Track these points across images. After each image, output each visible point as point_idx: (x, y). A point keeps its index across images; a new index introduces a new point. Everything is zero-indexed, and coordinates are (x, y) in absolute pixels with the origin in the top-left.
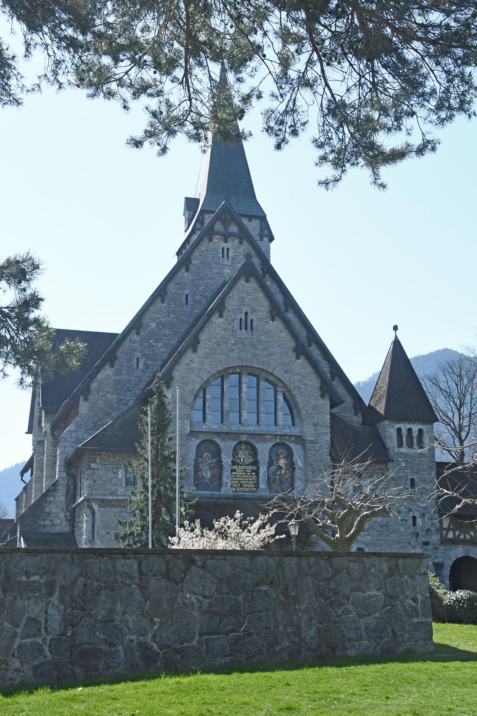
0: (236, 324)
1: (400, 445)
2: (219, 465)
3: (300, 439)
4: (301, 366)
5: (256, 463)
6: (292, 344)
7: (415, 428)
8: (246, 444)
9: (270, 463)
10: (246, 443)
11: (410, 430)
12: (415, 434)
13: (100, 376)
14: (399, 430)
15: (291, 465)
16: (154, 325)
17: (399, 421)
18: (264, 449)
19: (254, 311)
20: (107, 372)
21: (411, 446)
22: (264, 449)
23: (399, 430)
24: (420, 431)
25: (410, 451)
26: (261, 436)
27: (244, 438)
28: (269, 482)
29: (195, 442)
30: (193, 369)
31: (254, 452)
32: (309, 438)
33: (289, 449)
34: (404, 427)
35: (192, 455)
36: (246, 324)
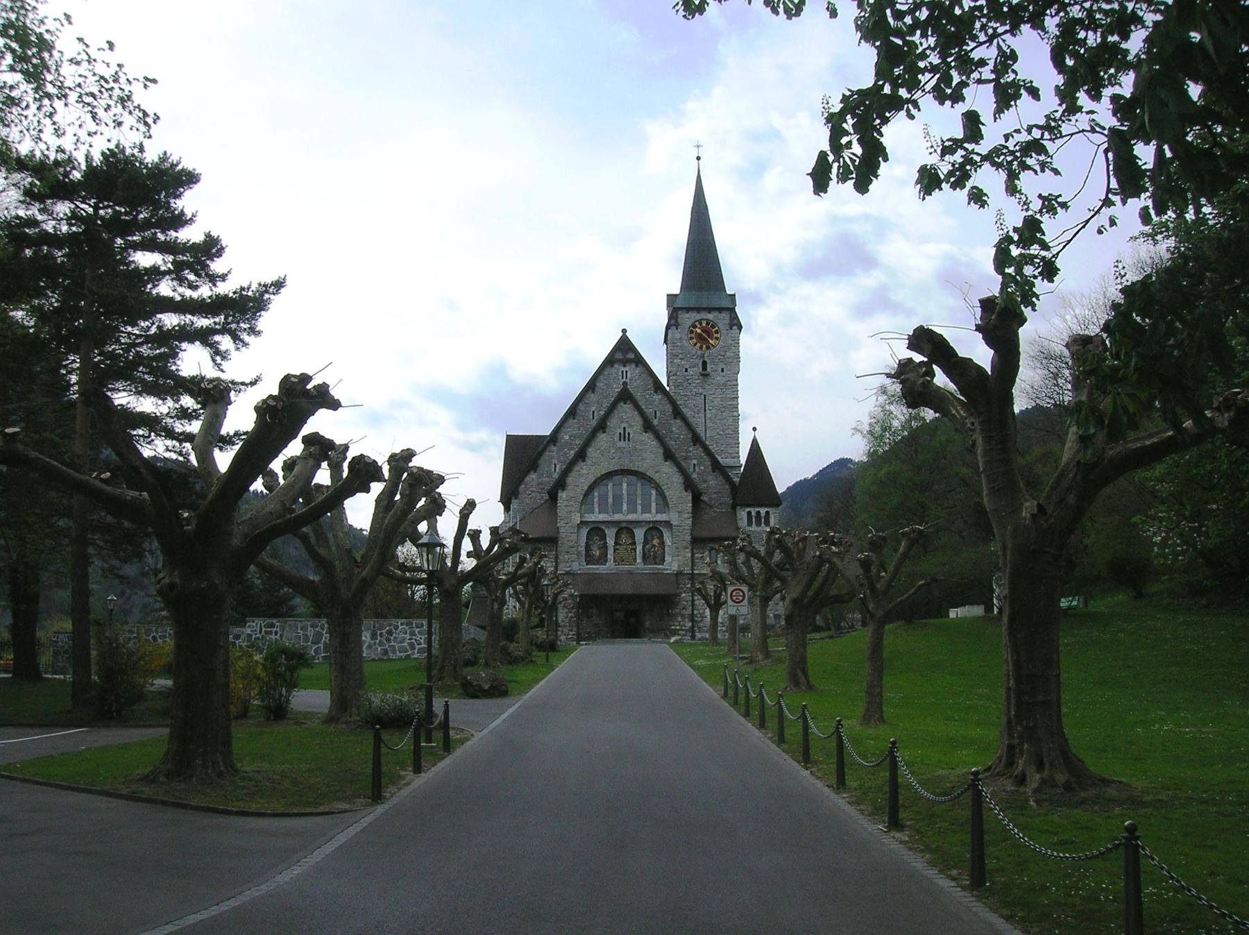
0: (616, 438)
1: (750, 523)
2: (605, 546)
3: (668, 524)
4: (668, 468)
5: (634, 543)
6: (661, 451)
7: (763, 511)
8: (625, 529)
9: (646, 542)
10: (627, 528)
11: (758, 513)
12: (763, 514)
13: (528, 479)
14: (749, 513)
15: (662, 543)
16: (567, 437)
17: (749, 506)
18: (639, 534)
19: (630, 426)
20: (532, 477)
21: (759, 524)
22: (639, 534)
23: (749, 513)
24: (767, 513)
25: (759, 529)
26: (638, 523)
27: (624, 525)
28: (644, 557)
29: (585, 532)
30: (583, 476)
31: (632, 535)
32: (674, 523)
33: (661, 532)
34: (754, 511)
35: (584, 539)
36: (624, 437)
